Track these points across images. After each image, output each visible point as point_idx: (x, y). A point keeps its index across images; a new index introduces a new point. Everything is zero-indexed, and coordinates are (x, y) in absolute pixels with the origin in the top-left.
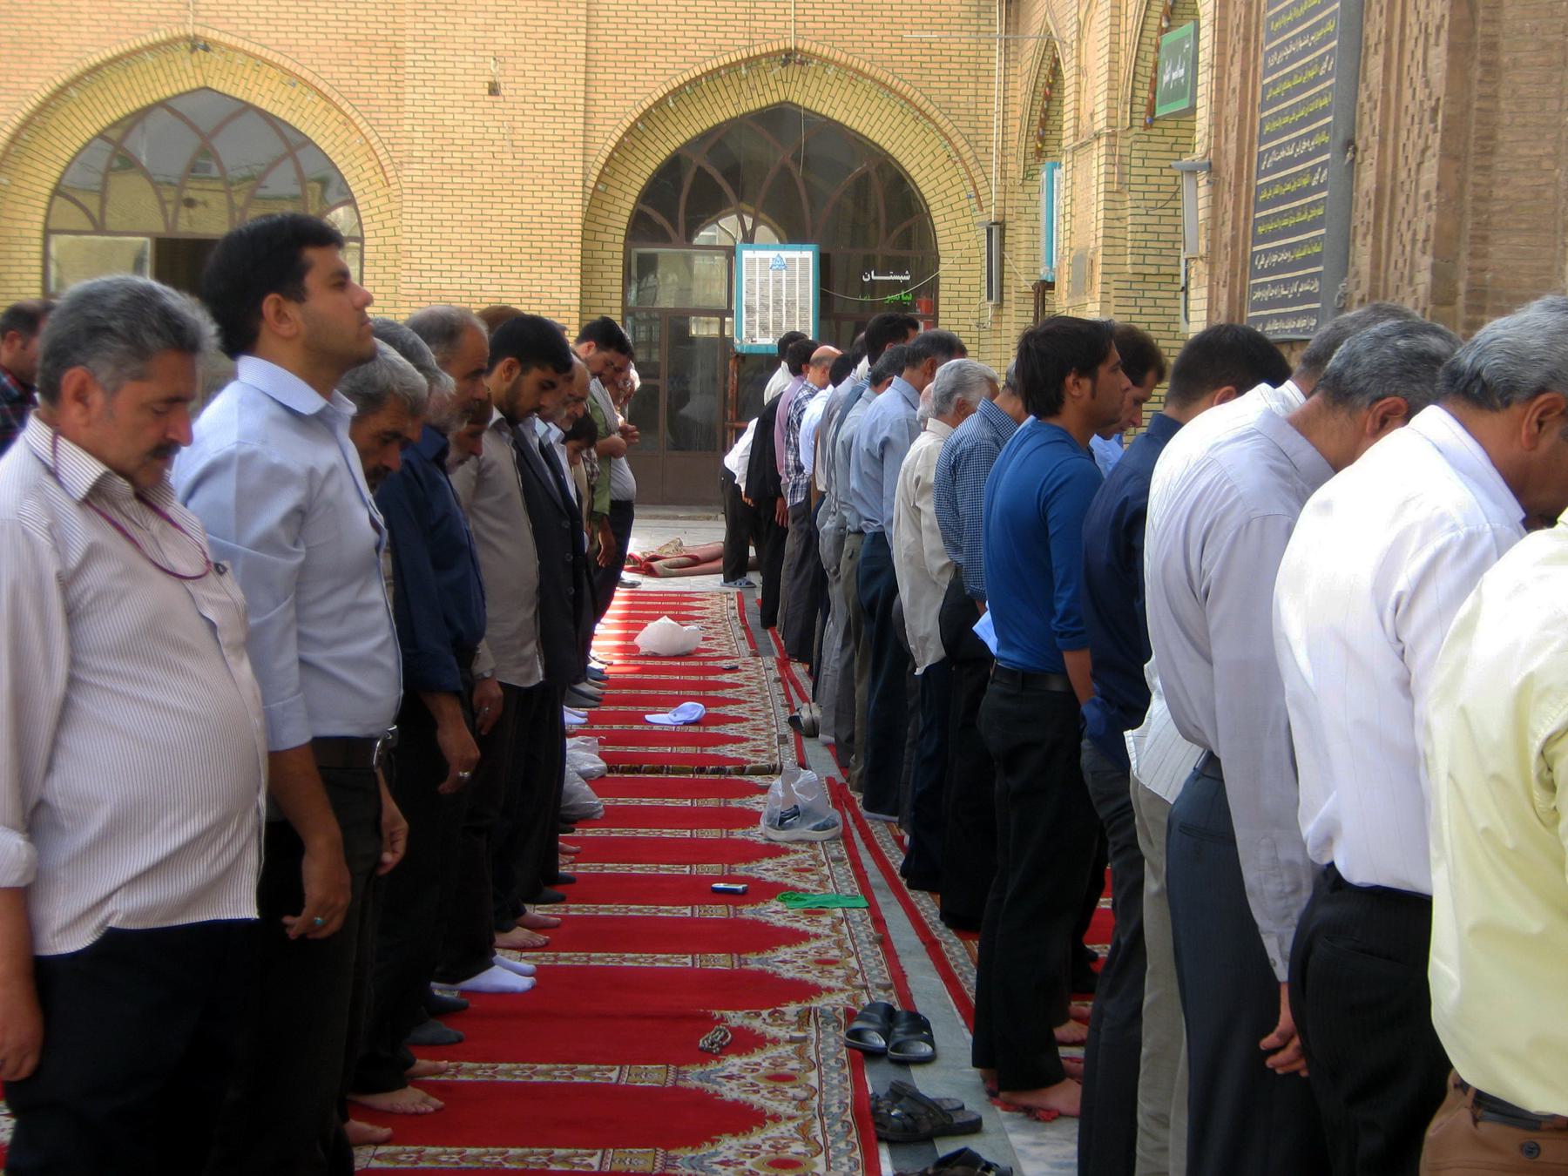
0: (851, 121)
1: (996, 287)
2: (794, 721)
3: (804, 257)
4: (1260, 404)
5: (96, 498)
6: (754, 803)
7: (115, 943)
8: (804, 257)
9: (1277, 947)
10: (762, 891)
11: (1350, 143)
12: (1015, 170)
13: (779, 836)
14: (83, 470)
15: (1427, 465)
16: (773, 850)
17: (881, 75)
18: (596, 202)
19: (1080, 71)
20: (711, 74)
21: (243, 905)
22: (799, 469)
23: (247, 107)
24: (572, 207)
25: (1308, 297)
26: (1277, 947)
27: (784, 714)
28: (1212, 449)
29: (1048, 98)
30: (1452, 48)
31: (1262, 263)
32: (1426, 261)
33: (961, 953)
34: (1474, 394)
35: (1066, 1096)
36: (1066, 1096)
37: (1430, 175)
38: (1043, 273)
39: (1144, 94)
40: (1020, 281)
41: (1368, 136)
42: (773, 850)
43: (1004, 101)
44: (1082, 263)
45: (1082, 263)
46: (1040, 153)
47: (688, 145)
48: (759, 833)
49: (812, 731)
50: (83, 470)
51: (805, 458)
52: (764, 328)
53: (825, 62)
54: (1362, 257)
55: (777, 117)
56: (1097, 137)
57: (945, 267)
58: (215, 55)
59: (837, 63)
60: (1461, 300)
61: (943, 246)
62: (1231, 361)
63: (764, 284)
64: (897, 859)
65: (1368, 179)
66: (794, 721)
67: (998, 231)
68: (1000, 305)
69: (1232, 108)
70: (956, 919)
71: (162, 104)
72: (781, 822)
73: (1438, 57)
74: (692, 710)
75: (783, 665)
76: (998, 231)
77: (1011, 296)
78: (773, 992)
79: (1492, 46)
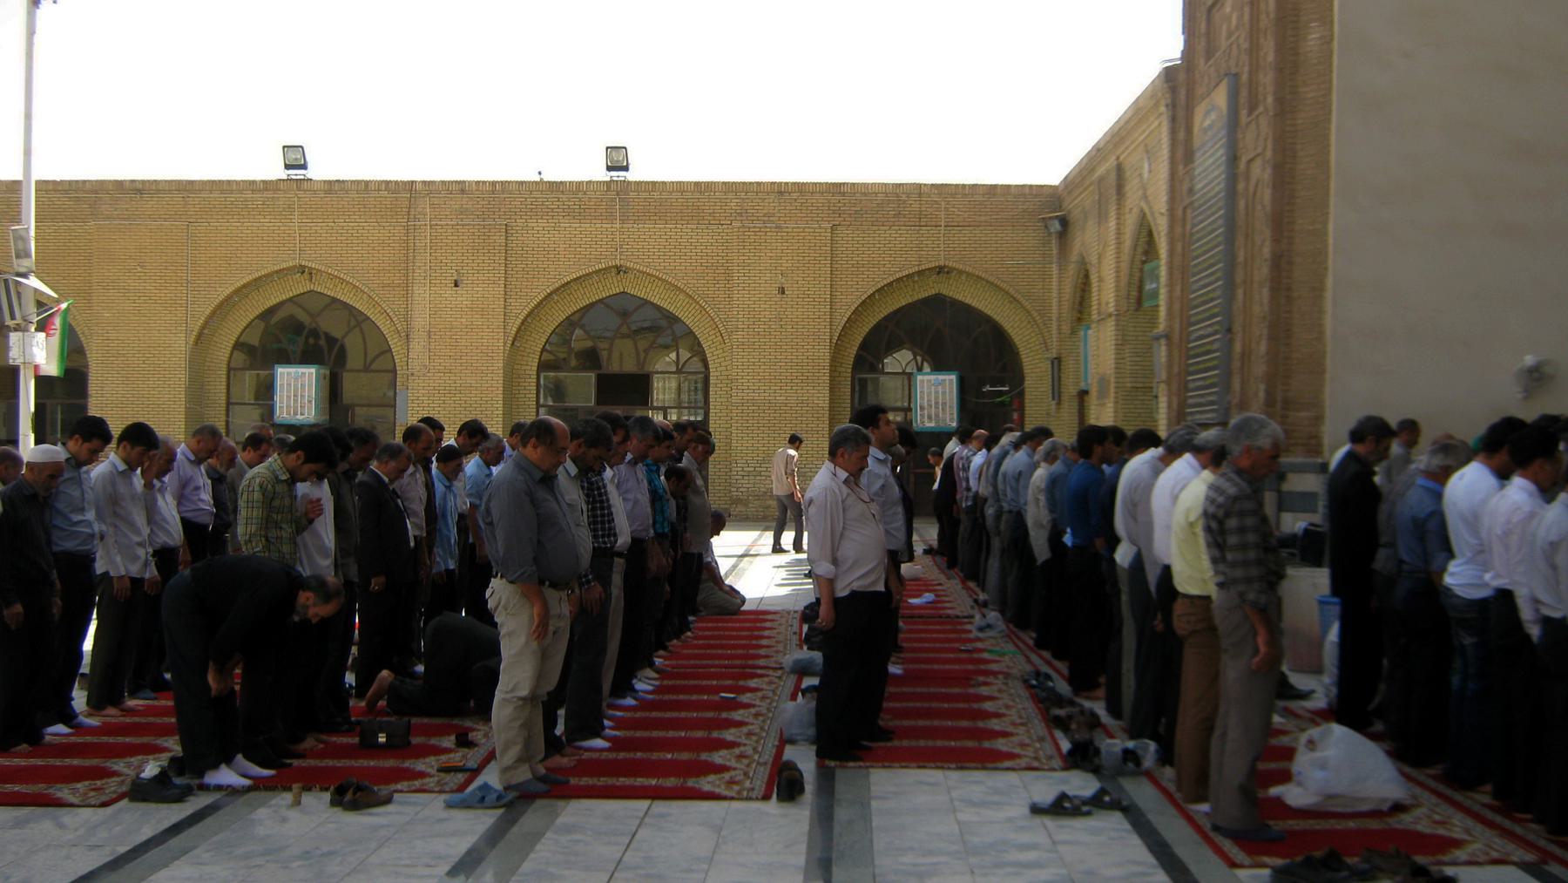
0: (975, 303)
1: (1057, 393)
2: (976, 601)
3: (951, 379)
4: (1152, 453)
5: (846, 482)
6: (968, 627)
7: (854, 595)
8: (951, 379)
9: (1153, 588)
10: (981, 650)
11: (1229, 330)
12: (1066, 328)
13: (981, 635)
14: (843, 475)
15: (1185, 464)
16: (979, 639)
17: (991, 279)
18: (837, 349)
19: (1101, 280)
20: (899, 280)
21: (881, 588)
22: (968, 489)
23: (646, 302)
24: (824, 354)
25: (1212, 403)
26: (1153, 588)
27: (970, 602)
28: (1138, 464)
29: (1083, 290)
30: (1272, 289)
31: (1191, 385)
32: (1262, 387)
33: (1063, 666)
34: (1197, 450)
35: (1101, 692)
36: (1101, 692)
37: (1263, 348)
38: (1083, 386)
39: (1134, 293)
40: (1070, 389)
41: (1237, 327)
42: (979, 639)
43: (1059, 291)
44: (1103, 381)
45: (1103, 381)
46: (1079, 320)
47: (886, 319)
48: (975, 634)
49: (985, 604)
50: (843, 475)
51: (973, 483)
52: (930, 417)
53: (960, 272)
54: (1236, 384)
55: (937, 302)
56: (1110, 315)
57: (1027, 383)
58: (630, 275)
59: (968, 274)
60: (1279, 405)
61: (1027, 369)
62: (1147, 439)
63: (929, 394)
64: (1031, 642)
65: (1238, 347)
66: (976, 601)
67: (1057, 362)
68: (1059, 403)
69: (1177, 307)
70: (1057, 656)
71: (600, 301)
72: (981, 629)
73: (1266, 292)
74: (929, 597)
75: (963, 583)
76: (1057, 362)
77: (1065, 397)
78: (995, 674)
79: (1289, 289)
